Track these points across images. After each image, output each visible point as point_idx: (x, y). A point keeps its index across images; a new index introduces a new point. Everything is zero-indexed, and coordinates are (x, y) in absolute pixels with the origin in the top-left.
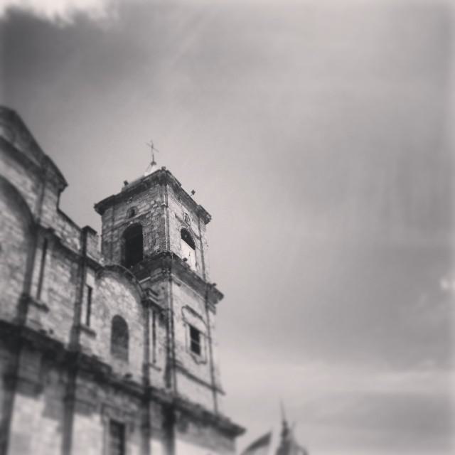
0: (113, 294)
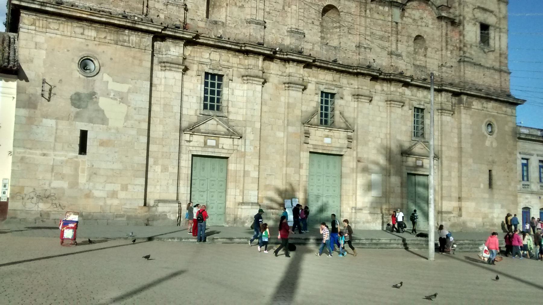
0: (414, 20)
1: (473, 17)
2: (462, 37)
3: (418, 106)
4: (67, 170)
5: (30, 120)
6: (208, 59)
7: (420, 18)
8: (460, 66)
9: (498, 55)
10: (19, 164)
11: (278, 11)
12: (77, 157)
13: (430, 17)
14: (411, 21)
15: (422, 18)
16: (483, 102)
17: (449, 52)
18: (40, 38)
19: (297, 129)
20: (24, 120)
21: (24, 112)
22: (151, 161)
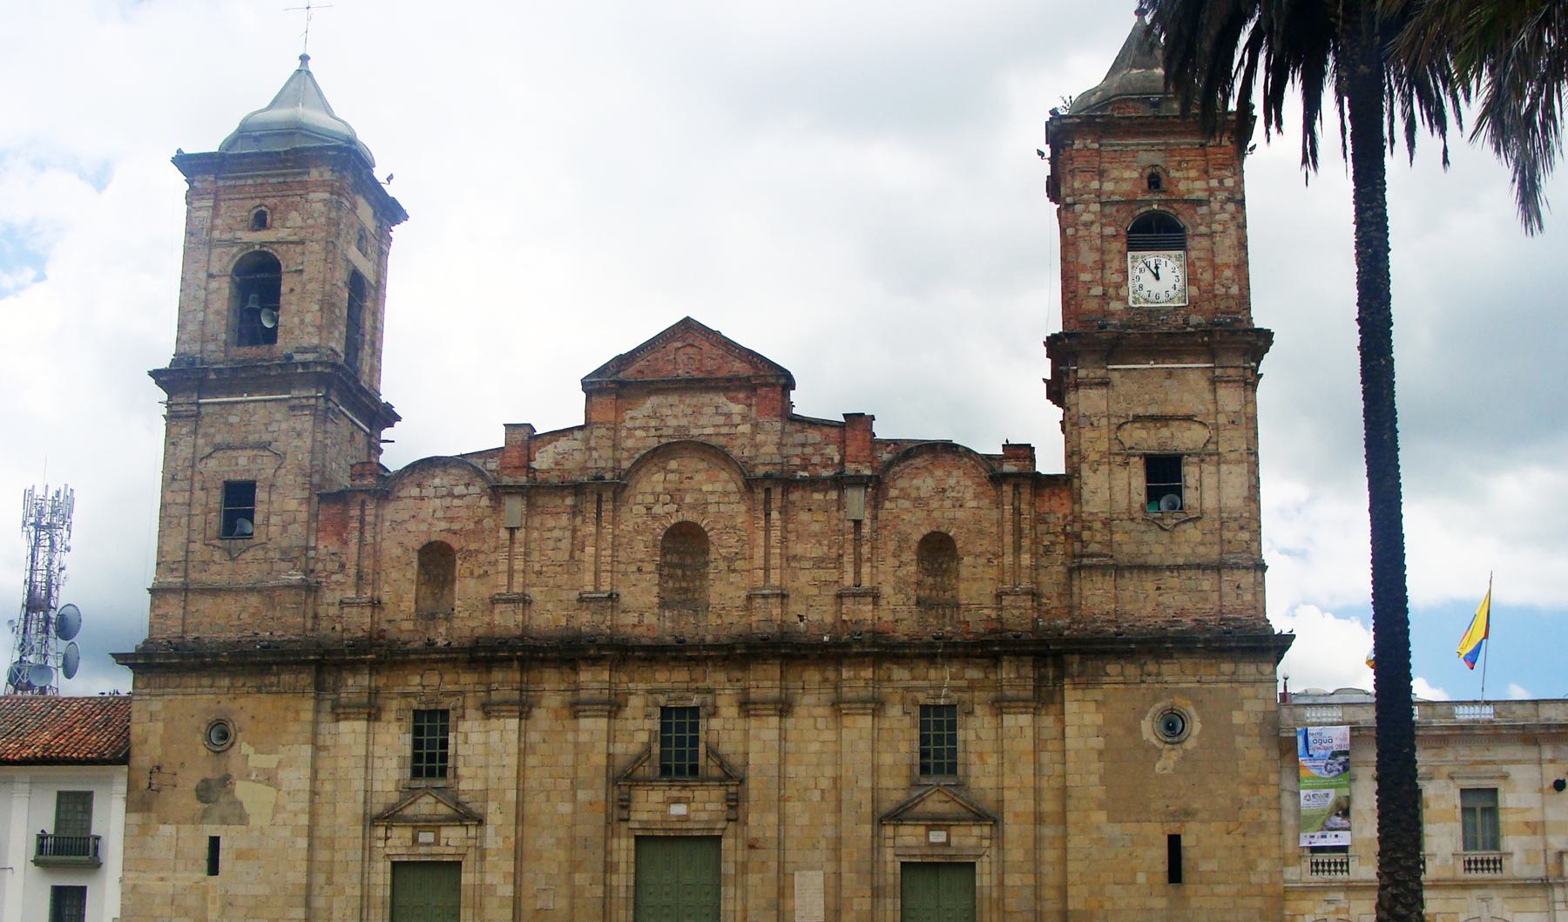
0: (919, 501)
1: (1116, 449)
2: (1077, 507)
3: (930, 702)
4: (191, 901)
5: (144, 829)
6: (418, 685)
7: (937, 493)
9: (1217, 525)
10: (130, 896)
11: (561, 565)
12: (205, 880)
13: (969, 483)
14: (907, 504)
15: (944, 490)
16: (1143, 661)
17: (1026, 559)
18: (156, 705)
19: (594, 793)
20: (136, 830)
21: (135, 818)
22: (321, 878)
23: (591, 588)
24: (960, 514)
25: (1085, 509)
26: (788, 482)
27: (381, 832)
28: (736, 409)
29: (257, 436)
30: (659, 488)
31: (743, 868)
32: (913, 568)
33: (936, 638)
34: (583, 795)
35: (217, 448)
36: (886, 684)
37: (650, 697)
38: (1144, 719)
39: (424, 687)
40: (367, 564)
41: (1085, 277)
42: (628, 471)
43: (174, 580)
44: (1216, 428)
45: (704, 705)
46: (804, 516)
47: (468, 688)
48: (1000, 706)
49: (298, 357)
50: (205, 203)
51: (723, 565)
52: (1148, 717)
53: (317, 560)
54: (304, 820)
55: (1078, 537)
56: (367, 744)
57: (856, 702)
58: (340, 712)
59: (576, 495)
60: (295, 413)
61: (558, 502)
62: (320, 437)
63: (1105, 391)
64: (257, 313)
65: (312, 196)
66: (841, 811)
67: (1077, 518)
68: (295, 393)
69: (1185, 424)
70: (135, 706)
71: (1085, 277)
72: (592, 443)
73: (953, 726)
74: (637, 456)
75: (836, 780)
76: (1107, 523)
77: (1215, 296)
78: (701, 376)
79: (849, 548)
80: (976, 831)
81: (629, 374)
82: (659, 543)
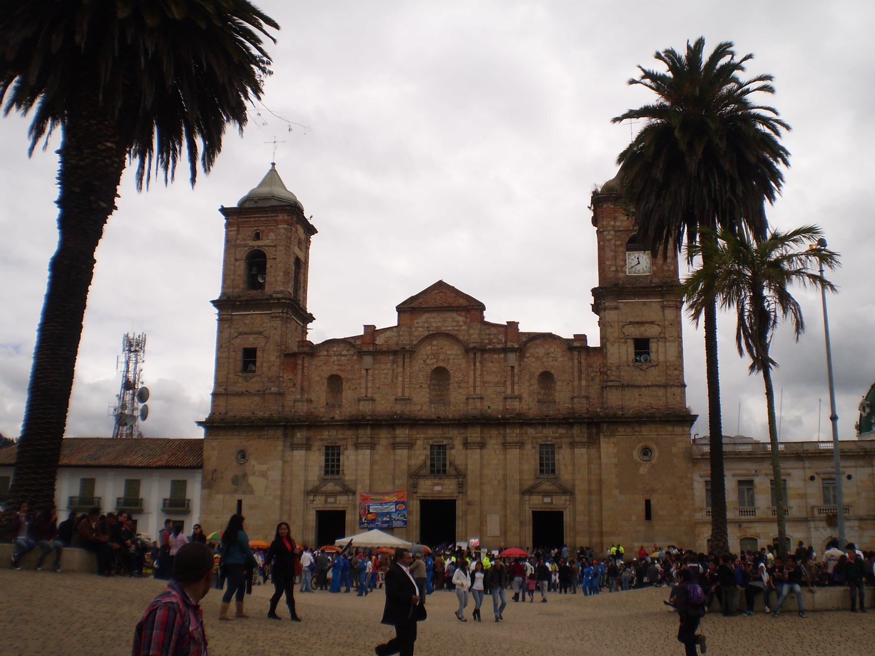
0: (538, 358)
2: (605, 360)
3: (544, 443)
8: (602, 391)
11: (388, 385)
13: (559, 350)
14: (533, 359)
15: (549, 354)
17: (584, 383)
18: (215, 443)
21: (206, 491)
23: (400, 395)
24: (555, 363)
25: (608, 361)
26: (484, 351)
27: (311, 498)
28: (461, 319)
29: (257, 328)
30: (429, 353)
31: (465, 513)
32: (536, 387)
33: (546, 416)
34: (397, 482)
35: (240, 334)
36: (525, 435)
37: (426, 441)
38: (634, 450)
39: (330, 436)
40: (306, 383)
41: (608, 263)
42: (416, 345)
43: (221, 390)
44: (664, 327)
45: (448, 444)
46: (490, 365)
47: (348, 437)
48: (573, 445)
49: (275, 296)
50: (233, 229)
51: (456, 385)
52: (636, 450)
53: (284, 382)
54: (278, 493)
55: (605, 373)
56: (306, 460)
57: (513, 443)
58: (294, 447)
59: (394, 355)
60: (274, 319)
61: (387, 358)
62: (284, 329)
63: (617, 311)
64: (256, 276)
65: (279, 226)
66: (506, 490)
67: (605, 365)
68: (273, 311)
69: (651, 325)
70: (205, 444)
71: (608, 263)
72: (401, 334)
73: (553, 453)
74: (420, 339)
75: (505, 476)
76: (618, 368)
77: (664, 270)
78: (446, 305)
79: (509, 378)
80: (563, 497)
81: (415, 304)
82: (429, 376)
